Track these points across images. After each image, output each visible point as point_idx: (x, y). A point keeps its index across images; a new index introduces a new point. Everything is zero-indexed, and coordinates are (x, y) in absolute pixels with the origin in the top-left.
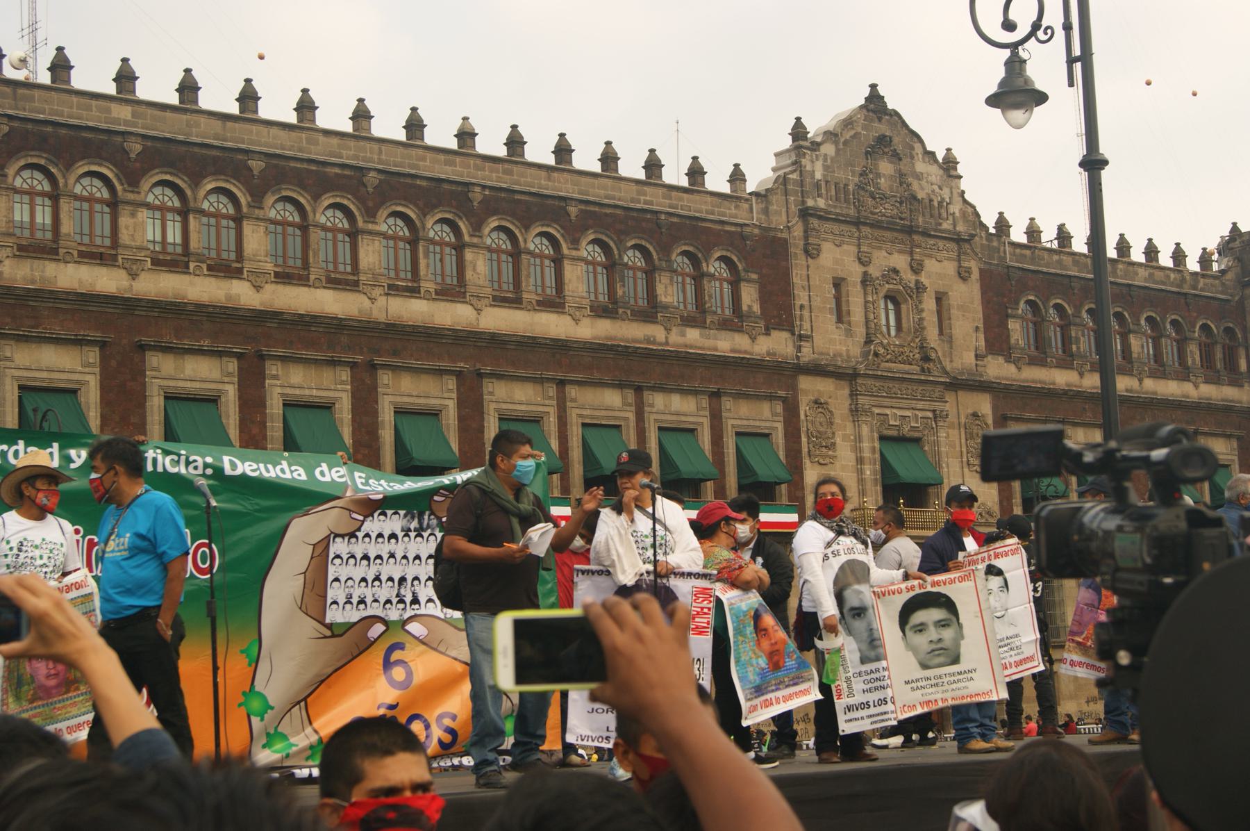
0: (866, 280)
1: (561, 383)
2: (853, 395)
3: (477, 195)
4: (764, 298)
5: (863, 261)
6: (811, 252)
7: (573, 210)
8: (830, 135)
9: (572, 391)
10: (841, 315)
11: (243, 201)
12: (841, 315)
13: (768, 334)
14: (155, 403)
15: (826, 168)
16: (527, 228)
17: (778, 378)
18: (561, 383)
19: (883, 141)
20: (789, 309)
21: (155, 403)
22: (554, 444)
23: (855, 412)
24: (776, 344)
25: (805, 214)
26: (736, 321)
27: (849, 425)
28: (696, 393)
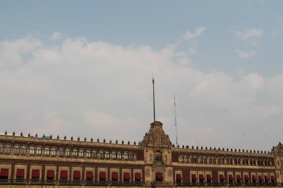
0: (281, 161)
1: (256, 172)
2: (281, 172)
3: (249, 156)
4: (272, 163)
5: (280, 159)
6: (275, 159)
7: (256, 157)
8: (276, 147)
9: (257, 173)
10: (279, 164)
11: (232, 158)
12: (279, 164)
13: (273, 166)
14: (228, 176)
15: (276, 151)
16: (253, 159)
17: (274, 171)
18: (256, 172)
19: (281, 147)
20: (274, 164)
21: (228, 176)
22: (256, 178)
23: (281, 173)
24: (273, 168)
25: (275, 155)
26: (269, 165)
27: (280, 175)
28: (267, 172)
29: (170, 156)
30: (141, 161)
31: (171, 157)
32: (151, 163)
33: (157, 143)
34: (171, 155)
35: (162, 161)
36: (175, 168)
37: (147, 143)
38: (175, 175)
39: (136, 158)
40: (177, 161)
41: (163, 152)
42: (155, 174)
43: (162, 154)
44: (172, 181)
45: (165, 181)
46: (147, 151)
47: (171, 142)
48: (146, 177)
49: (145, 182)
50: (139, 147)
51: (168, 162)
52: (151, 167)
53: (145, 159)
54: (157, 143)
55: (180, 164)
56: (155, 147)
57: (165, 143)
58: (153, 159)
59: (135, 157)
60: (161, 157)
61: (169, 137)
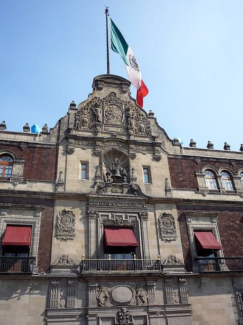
29: (161, 170)
30: (39, 184)
31: (167, 173)
32: (85, 188)
33: (111, 129)
34: (167, 167)
35: (133, 183)
36: (187, 209)
37: (71, 126)
38: (191, 232)
39: (21, 172)
40: (196, 188)
41: (133, 157)
42: (101, 230)
43: (130, 160)
44: (180, 256)
45: (147, 255)
46: (68, 152)
47: (163, 130)
48: (55, 241)
49: (54, 261)
50: (42, 138)
51: (158, 186)
52: (84, 203)
53: (58, 175)
54: (111, 129)
55: (204, 195)
56: (102, 140)
57: (140, 129)
58: (93, 176)
59: (18, 169)
60: (128, 171)
61: (155, 116)
